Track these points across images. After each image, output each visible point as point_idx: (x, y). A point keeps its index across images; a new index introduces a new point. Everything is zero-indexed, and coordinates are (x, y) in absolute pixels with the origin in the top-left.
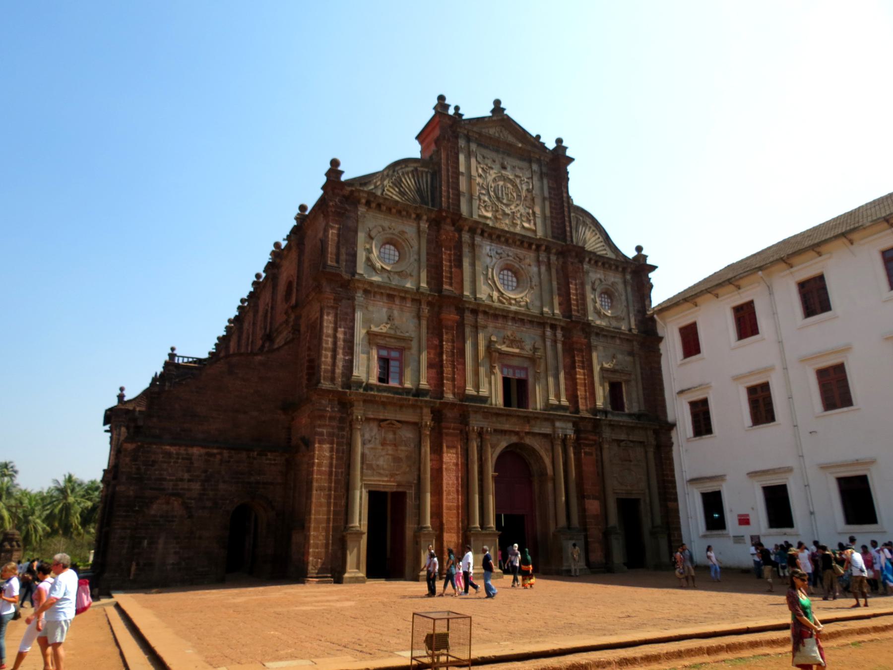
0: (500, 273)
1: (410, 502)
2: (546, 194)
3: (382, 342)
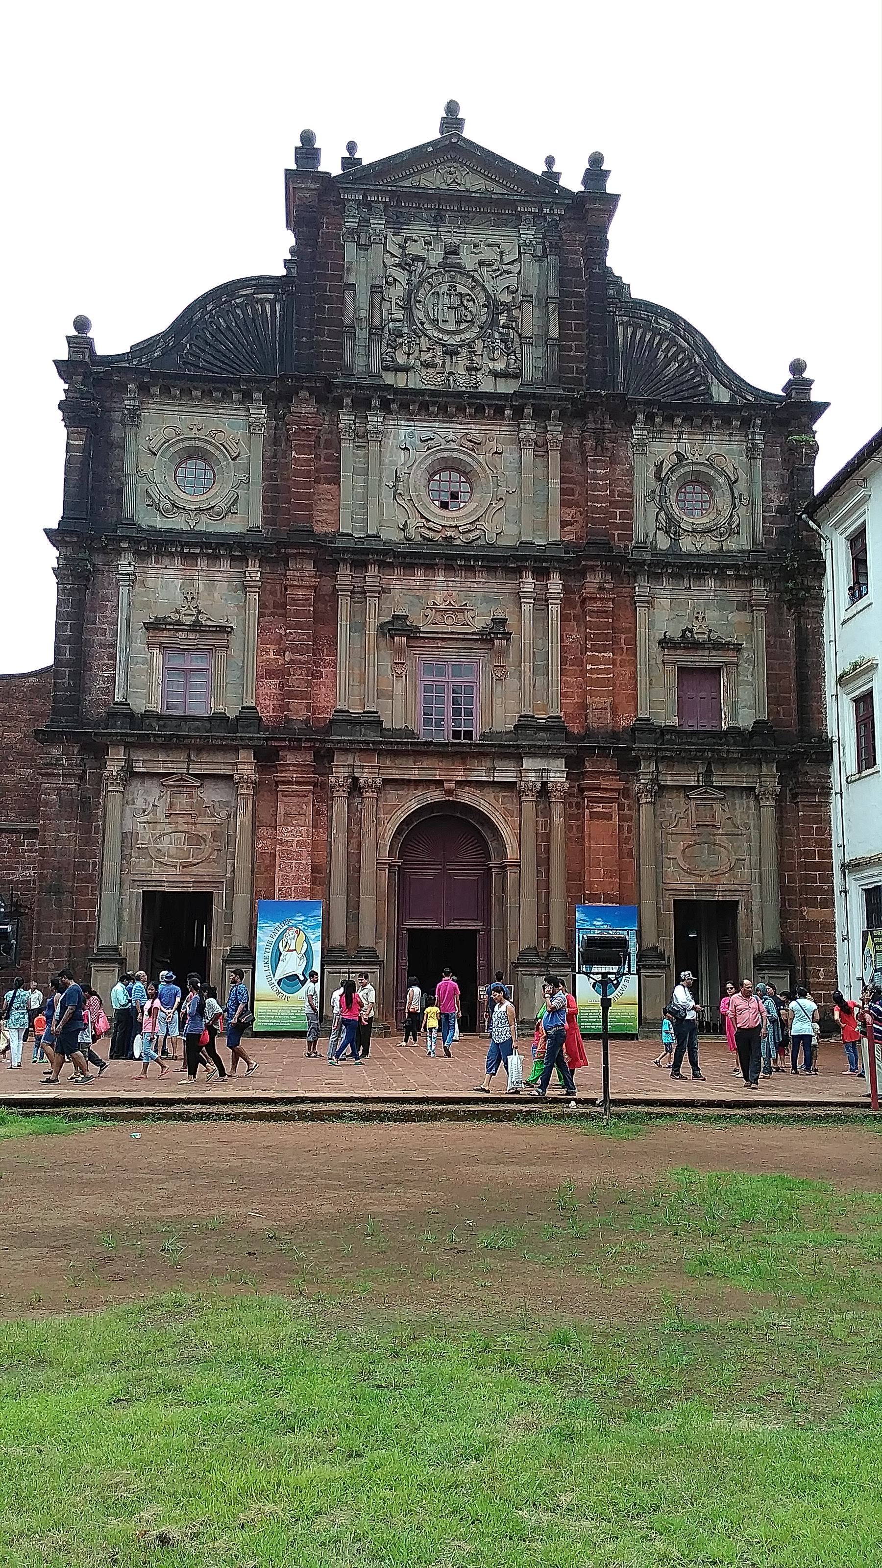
1: (218, 909)
2: (553, 291)
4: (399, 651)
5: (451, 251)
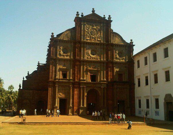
3: (63, 70)
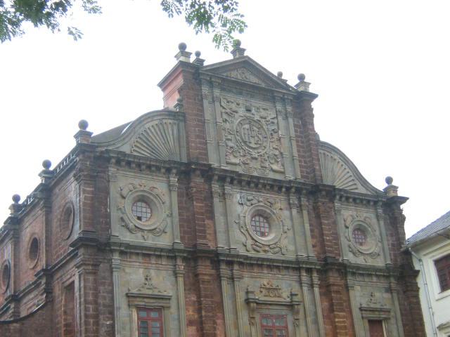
0: (252, 220)
2: (293, 133)
4: (251, 311)
5: (249, 110)
